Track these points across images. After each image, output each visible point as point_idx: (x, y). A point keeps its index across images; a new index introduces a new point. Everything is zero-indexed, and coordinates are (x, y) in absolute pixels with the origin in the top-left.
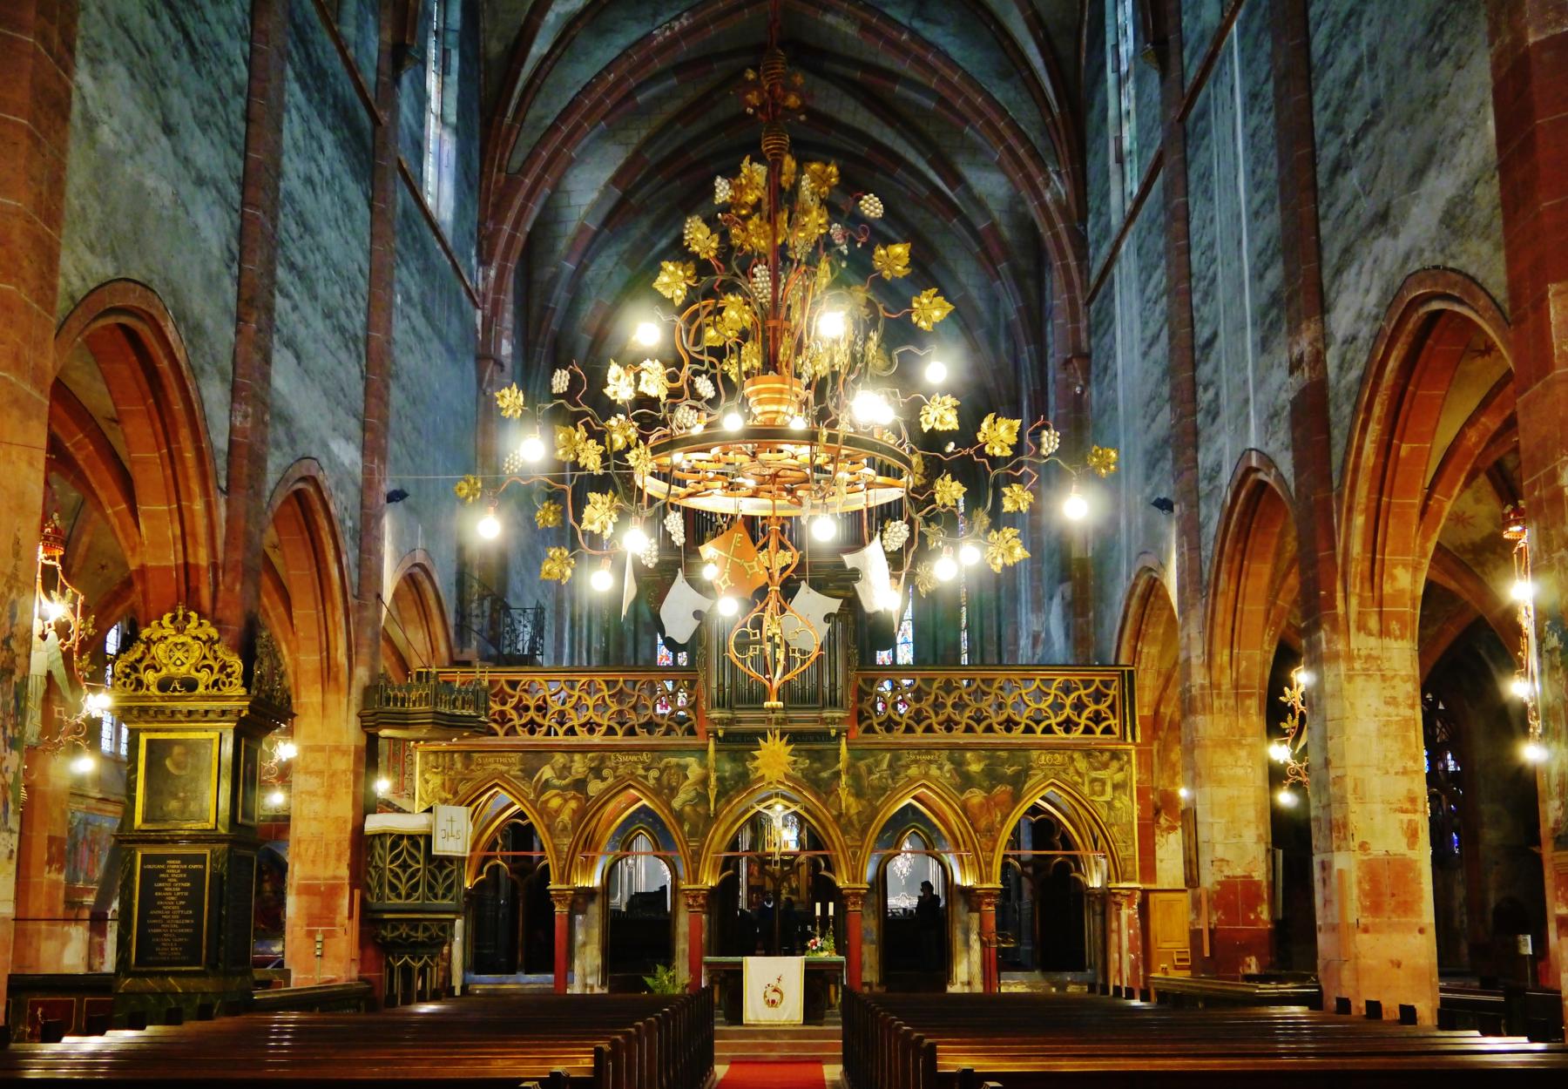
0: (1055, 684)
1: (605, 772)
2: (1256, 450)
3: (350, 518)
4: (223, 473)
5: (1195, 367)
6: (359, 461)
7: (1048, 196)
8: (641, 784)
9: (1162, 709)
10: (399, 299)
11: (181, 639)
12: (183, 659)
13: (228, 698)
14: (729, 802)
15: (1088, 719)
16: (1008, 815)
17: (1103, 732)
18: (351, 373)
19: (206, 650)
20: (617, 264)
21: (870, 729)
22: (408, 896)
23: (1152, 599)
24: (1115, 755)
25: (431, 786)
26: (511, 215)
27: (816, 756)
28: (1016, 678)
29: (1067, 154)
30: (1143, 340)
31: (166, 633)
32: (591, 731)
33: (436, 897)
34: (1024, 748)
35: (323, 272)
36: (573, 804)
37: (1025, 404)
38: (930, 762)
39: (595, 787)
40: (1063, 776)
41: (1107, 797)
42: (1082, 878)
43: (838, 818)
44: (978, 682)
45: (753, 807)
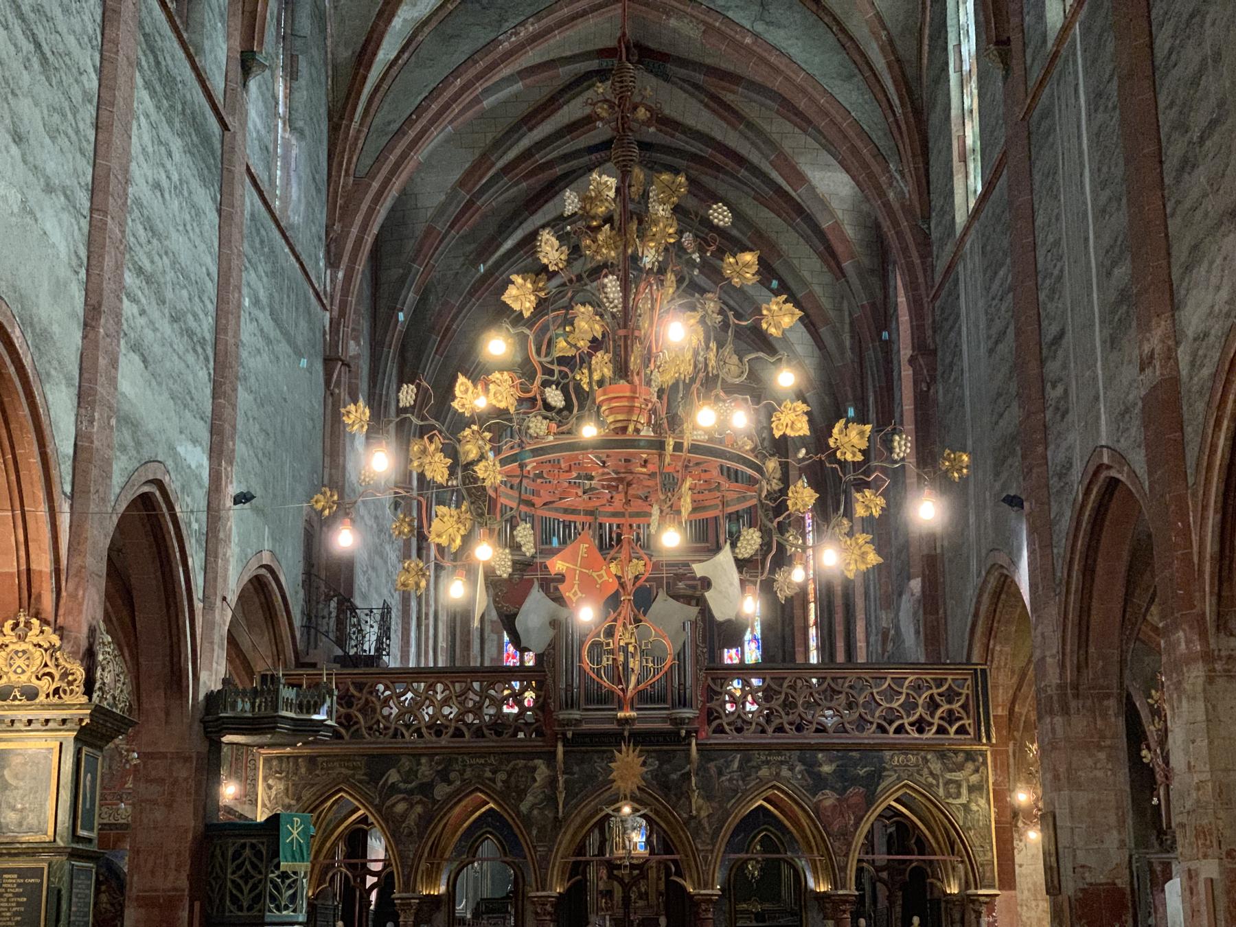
0: (907, 682)
1: (452, 775)
2: (1108, 447)
3: (197, 521)
4: (68, 478)
5: (1042, 363)
6: (206, 463)
7: (891, 195)
8: (489, 787)
9: (1017, 709)
10: (247, 302)
11: (23, 646)
12: (24, 667)
13: (70, 707)
14: (576, 806)
15: (941, 718)
16: (862, 819)
17: (957, 732)
18: (200, 377)
19: (47, 658)
21: (720, 730)
23: (1003, 596)
24: (970, 756)
25: (274, 792)
26: (359, 219)
27: (664, 758)
28: (867, 677)
29: (909, 154)
30: (989, 337)
31: (6, 640)
32: (439, 733)
34: (878, 748)
35: (170, 275)
36: (419, 809)
37: (871, 399)
38: (782, 763)
39: (441, 791)
40: (918, 777)
41: (964, 800)
42: (939, 884)
43: (686, 823)
44: (829, 680)
45: (602, 810)
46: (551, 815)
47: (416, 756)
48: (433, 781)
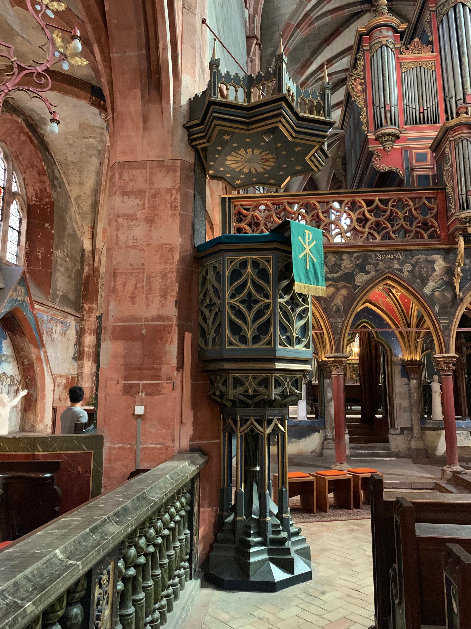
1: (368, 268)
20: (294, 75)
22: (256, 339)
33: (290, 341)
36: (344, 292)
39: (360, 279)
46: (449, 295)
47: (340, 254)
48: (353, 271)
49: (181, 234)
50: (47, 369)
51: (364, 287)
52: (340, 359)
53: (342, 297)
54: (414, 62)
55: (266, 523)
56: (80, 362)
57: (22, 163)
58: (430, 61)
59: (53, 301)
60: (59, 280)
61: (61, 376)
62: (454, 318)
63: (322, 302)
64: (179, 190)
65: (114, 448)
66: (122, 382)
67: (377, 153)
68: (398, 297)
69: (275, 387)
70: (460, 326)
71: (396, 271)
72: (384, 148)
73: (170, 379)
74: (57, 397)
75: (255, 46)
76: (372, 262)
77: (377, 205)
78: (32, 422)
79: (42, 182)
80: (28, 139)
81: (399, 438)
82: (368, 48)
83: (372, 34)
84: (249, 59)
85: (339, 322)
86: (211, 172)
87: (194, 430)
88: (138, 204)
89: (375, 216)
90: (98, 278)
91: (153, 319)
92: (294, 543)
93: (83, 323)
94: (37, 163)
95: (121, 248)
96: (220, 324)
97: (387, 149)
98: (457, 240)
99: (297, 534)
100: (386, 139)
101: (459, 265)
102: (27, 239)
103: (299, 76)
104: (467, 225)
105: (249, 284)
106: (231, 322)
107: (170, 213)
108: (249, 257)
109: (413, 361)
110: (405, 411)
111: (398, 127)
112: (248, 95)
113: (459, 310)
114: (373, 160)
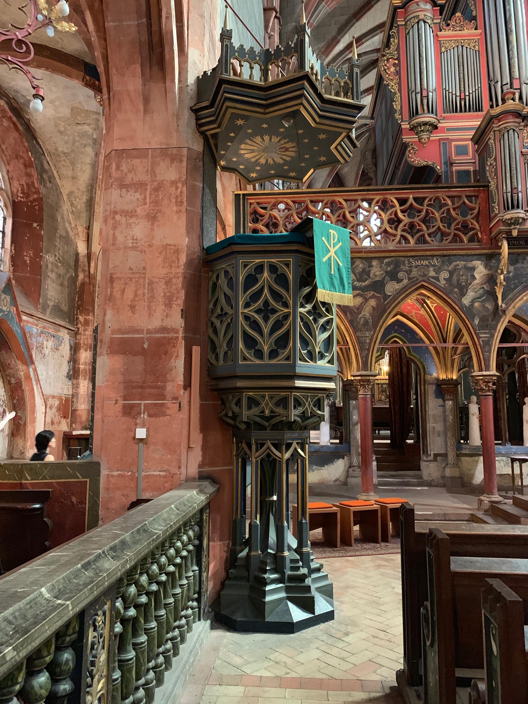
1: (400, 275)
33: (311, 356)
36: (373, 302)
39: (391, 288)
46: (490, 306)
47: (369, 260)
48: (384, 279)
49: (188, 233)
50: (37, 389)
51: (395, 298)
52: (368, 378)
53: (371, 308)
54: (455, 40)
55: (284, 558)
56: (75, 381)
57: (5, 152)
58: (473, 39)
59: (44, 311)
60: (50, 287)
61: (54, 397)
62: (495, 332)
63: (348, 314)
64: (185, 183)
65: (113, 476)
66: (121, 402)
67: (412, 144)
68: (433, 309)
69: (295, 407)
70: (501, 341)
71: (431, 279)
72: (419, 140)
73: (176, 398)
74: (49, 420)
75: (274, 20)
76: (405, 269)
77: (412, 204)
78: (21, 449)
79: (29, 175)
80: (12, 125)
81: (432, 465)
82: (403, 23)
83: (408, 7)
84: (267, 35)
85: (367, 337)
86: (222, 163)
87: (204, 456)
88: (138, 199)
89: (409, 216)
90: (94, 286)
91: (157, 331)
92: (315, 580)
93: (78, 337)
94: (23, 152)
95: (119, 249)
96: (232, 336)
97: (423, 140)
98: (500, 244)
99: (318, 570)
100: (422, 129)
101: (502, 273)
102: (13, 241)
103: (324, 57)
104: (512, 227)
105: (266, 291)
106: (245, 334)
107: (175, 209)
108: (266, 260)
109: (449, 380)
110: (439, 436)
111: (436, 115)
112: (265, 73)
113: (500, 323)
114: (407, 153)
